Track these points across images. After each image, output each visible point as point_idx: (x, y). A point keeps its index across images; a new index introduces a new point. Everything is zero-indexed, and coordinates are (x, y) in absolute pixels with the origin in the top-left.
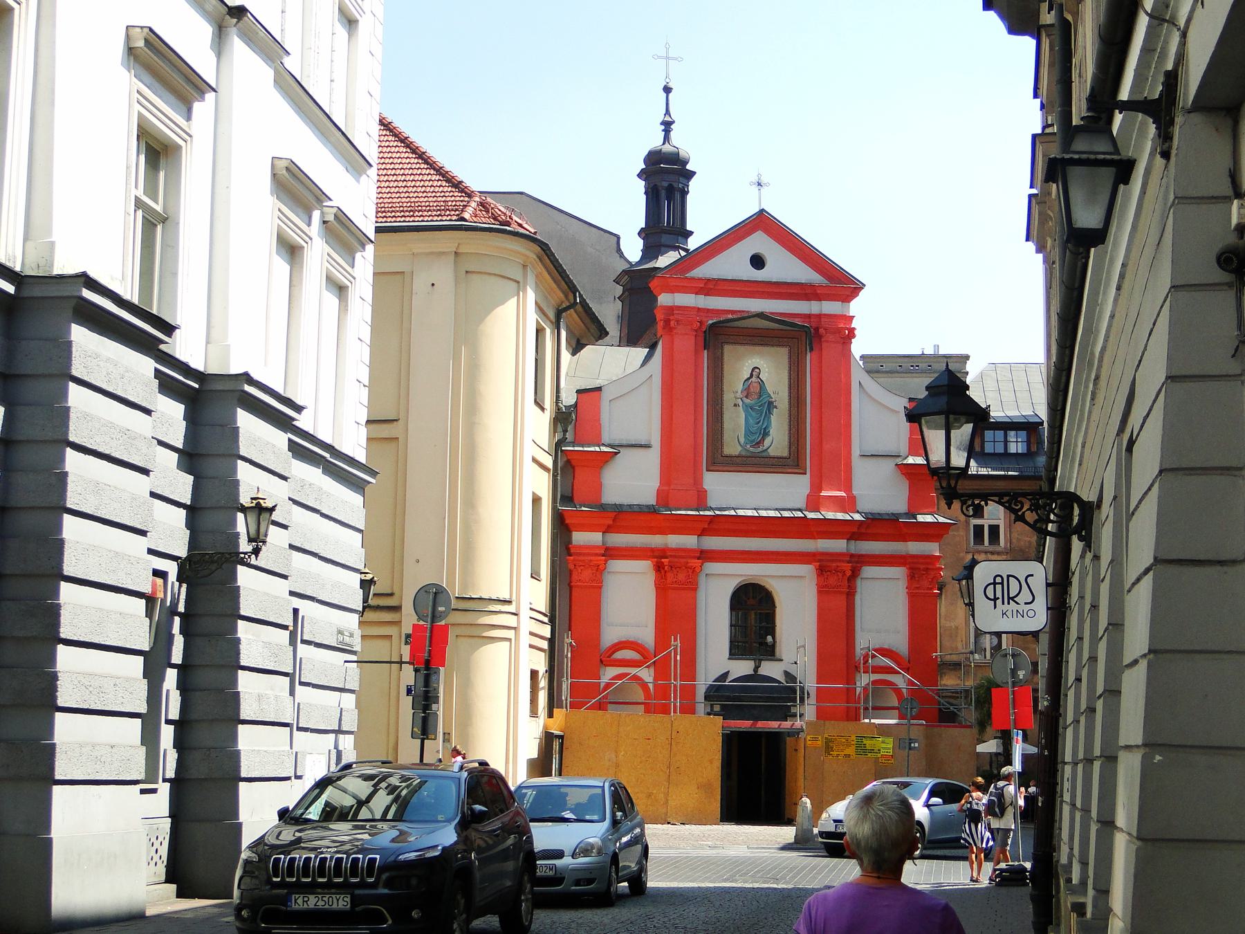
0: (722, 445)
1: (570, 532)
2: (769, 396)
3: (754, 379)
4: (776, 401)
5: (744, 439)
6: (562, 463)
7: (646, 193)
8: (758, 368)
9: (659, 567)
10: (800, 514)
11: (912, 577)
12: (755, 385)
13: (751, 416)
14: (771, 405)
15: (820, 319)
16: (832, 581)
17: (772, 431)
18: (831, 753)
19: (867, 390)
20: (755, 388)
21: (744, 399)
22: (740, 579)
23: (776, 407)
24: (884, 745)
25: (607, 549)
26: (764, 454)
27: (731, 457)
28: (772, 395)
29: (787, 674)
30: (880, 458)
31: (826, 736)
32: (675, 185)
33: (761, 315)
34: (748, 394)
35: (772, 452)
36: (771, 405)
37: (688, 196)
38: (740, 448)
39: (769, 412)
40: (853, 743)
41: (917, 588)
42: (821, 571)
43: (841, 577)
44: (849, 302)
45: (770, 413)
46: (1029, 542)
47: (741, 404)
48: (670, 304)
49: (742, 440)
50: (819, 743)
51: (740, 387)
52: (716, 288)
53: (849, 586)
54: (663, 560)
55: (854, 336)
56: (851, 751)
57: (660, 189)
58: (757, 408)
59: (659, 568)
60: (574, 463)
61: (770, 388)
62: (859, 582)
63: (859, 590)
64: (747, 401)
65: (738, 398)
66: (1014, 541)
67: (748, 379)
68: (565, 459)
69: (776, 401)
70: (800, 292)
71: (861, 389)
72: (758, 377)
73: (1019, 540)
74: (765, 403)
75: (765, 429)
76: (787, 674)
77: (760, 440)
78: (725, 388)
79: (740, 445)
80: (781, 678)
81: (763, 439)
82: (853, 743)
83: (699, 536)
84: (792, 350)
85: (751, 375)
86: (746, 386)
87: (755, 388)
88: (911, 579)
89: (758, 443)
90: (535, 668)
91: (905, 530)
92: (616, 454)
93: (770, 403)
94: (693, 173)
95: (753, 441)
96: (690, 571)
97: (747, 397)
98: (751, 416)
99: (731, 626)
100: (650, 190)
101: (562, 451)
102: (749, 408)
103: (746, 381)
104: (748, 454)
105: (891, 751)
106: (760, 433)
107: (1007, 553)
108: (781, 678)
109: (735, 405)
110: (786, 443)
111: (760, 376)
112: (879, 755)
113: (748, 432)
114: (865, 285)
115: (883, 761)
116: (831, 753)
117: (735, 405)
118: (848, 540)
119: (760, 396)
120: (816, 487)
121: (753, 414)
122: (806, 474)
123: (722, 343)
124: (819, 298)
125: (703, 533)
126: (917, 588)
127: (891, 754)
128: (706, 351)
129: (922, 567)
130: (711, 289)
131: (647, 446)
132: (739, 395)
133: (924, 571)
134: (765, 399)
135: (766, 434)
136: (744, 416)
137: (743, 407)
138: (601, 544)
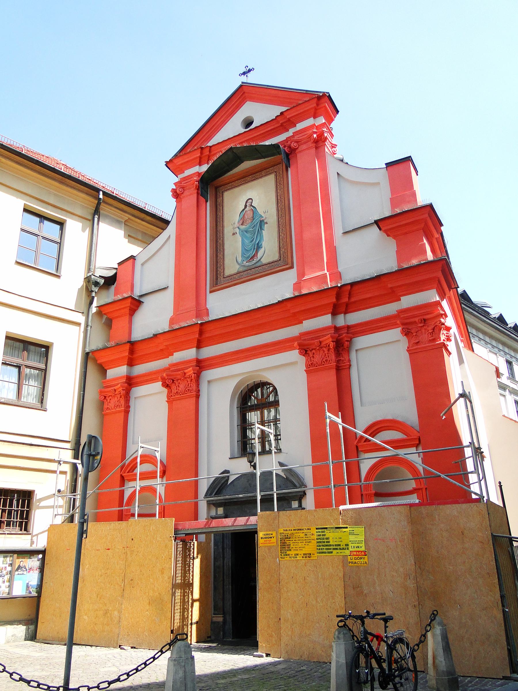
0: (224, 269)
2: (261, 217)
3: (248, 208)
5: (241, 258)
8: (252, 199)
13: (246, 237)
14: (262, 223)
16: (318, 358)
17: (264, 244)
18: (288, 552)
19: (346, 177)
20: (249, 214)
23: (267, 223)
24: (352, 538)
26: (259, 264)
28: (263, 215)
31: (281, 531)
34: (243, 222)
35: (264, 261)
36: (262, 223)
38: (238, 267)
39: (261, 228)
40: (312, 537)
42: (305, 351)
43: (326, 352)
47: (237, 230)
49: (240, 259)
50: (274, 540)
56: (311, 548)
58: (251, 229)
61: (260, 211)
63: (354, 363)
65: (236, 228)
67: (244, 210)
72: (251, 205)
74: (258, 222)
75: (258, 244)
77: (255, 254)
79: (239, 264)
81: (257, 252)
82: (312, 537)
89: (252, 258)
95: (249, 256)
97: (242, 224)
98: (246, 237)
102: (244, 233)
104: (245, 269)
105: (363, 544)
106: (254, 248)
109: (234, 234)
110: (276, 249)
111: (252, 205)
112: (347, 552)
113: (245, 251)
115: (354, 561)
116: (288, 552)
117: (234, 234)
119: (253, 219)
120: (301, 274)
121: (248, 235)
127: (363, 549)
132: (236, 225)
133: (421, 323)
134: (257, 220)
135: (258, 247)
137: (239, 233)
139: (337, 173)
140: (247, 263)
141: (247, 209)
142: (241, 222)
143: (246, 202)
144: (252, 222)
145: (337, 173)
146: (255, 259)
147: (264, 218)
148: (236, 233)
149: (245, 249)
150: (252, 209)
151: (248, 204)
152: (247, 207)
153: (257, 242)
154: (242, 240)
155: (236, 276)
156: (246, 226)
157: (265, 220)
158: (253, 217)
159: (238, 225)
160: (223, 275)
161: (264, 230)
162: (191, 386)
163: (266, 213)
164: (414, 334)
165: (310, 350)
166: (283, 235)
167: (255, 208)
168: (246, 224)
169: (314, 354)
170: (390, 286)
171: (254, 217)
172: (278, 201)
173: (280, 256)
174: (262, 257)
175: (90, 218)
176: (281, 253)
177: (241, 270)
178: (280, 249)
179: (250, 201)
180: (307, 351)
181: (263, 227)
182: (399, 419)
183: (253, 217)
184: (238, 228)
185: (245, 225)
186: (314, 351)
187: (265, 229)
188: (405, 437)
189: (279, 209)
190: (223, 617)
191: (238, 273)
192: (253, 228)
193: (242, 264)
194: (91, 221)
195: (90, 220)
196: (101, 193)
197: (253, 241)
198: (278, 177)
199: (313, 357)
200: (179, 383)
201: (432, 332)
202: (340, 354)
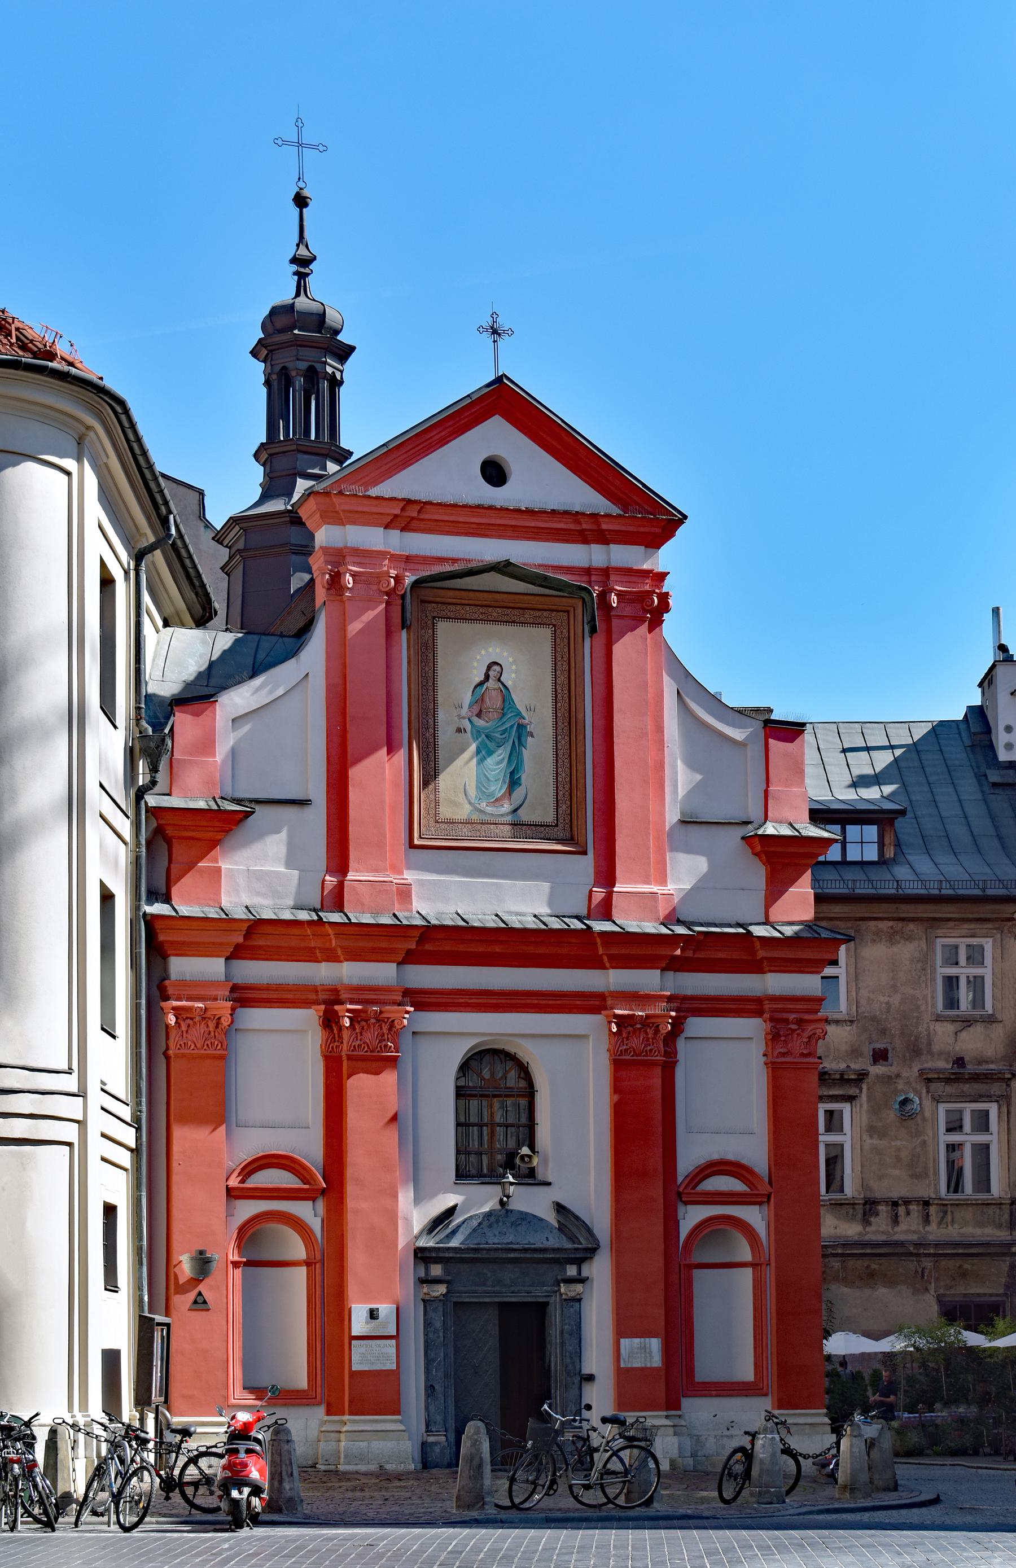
1: (165, 957)
3: (491, 684)
6: (149, 833)
7: (268, 383)
8: (501, 666)
9: (329, 1020)
10: (577, 925)
11: (774, 1037)
12: (494, 693)
15: (608, 577)
20: (493, 701)
21: (475, 719)
23: (532, 736)
25: (235, 988)
27: (451, 822)
28: (524, 713)
29: (560, 1208)
30: (714, 828)
32: (318, 366)
33: (504, 568)
34: (481, 711)
37: (342, 389)
38: (468, 808)
41: (783, 1054)
44: (658, 547)
46: (887, 1003)
47: (468, 727)
48: (340, 544)
49: (472, 793)
51: (467, 698)
52: (422, 516)
53: (665, 1051)
54: (336, 1007)
55: (667, 609)
57: (293, 373)
58: (498, 735)
59: (329, 1021)
60: (170, 832)
62: (681, 1044)
63: (680, 1056)
64: (480, 723)
65: (464, 718)
66: (863, 1002)
68: (154, 824)
70: (572, 526)
72: (499, 680)
73: (870, 1000)
74: (512, 727)
76: (560, 1208)
78: (441, 698)
79: (470, 803)
83: (399, 964)
84: (558, 631)
85: (487, 677)
86: (477, 696)
87: (493, 701)
88: (773, 1039)
90: (112, 1201)
91: (761, 954)
92: (248, 815)
93: (521, 727)
94: (352, 349)
95: (492, 795)
96: (385, 1028)
97: (479, 715)
99: (458, 1124)
100: (274, 377)
101: (148, 809)
103: (475, 687)
107: (852, 1022)
108: (551, 1217)
109: (459, 730)
111: (502, 679)
114: (685, 517)
117: (459, 730)
118: (663, 970)
119: (504, 714)
122: (585, 853)
123: (434, 618)
124: (603, 538)
125: (410, 958)
126: (783, 1054)
128: (404, 633)
129: (792, 1017)
130: (413, 519)
131: (303, 803)
138: (223, 979)
142: (476, 710)
143: (489, 668)
144: (501, 718)
146: (505, 805)
147: (527, 722)
149: (485, 775)
150: (501, 691)
151: (491, 673)
155: (465, 830)
156: (487, 722)
158: (503, 710)
159: (469, 713)
160: (436, 816)
162: (388, 1039)
163: (532, 712)
164: (783, 1038)
166: (564, 775)
167: (508, 689)
169: (629, 1033)
171: (505, 710)
172: (556, 697)
173: (557, 817)
174: (521, 806)
176: (560, 812)
177: (475, 817)
178: (557, 803)
179: (497, 668)
181: (523, 739)
182: (744, 1162)
183: (503, 710)
184: (469, 720)
185: (484, 720)
187: (528, 746)
188: (748, 1190)
189: (559, 715)
190: (445, 1435)
191: (467, 822)
193: (478, 806)
198: (558, 640)
200: (363, 1027)
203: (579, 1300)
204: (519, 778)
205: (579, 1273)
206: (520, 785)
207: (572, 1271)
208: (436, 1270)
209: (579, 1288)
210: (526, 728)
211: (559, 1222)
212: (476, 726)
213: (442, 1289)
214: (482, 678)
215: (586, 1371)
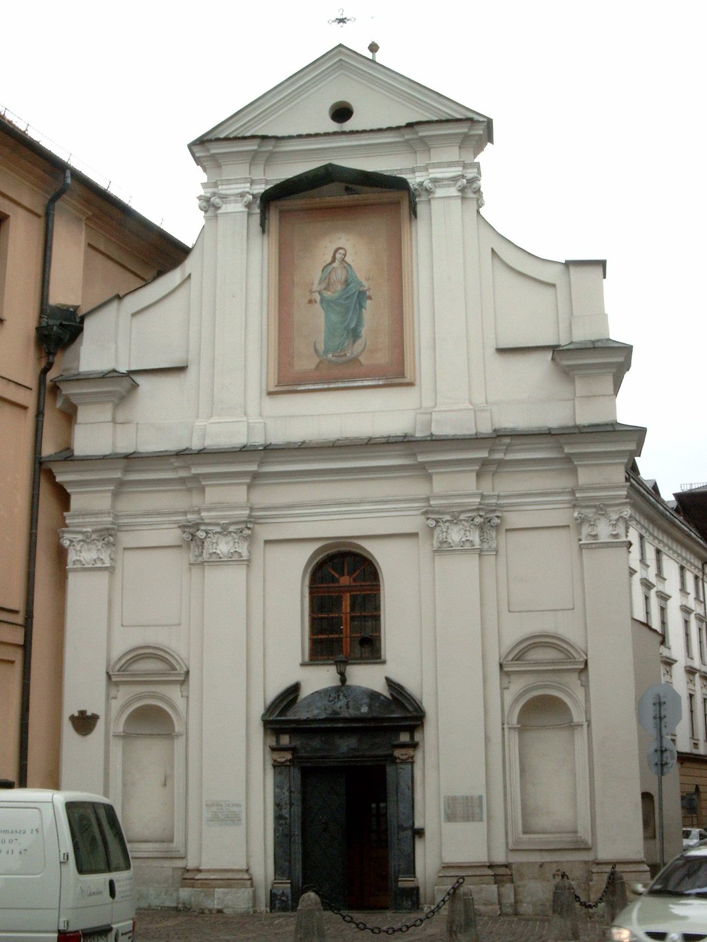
4: (369, 289)
8: (346, 251)
14: (362, 296)
17: (364, 331)
20: (339, 275)
21: (324, 292)
22: (318, 545)
23: (370, 298)
28: (365, 283)
29: (390, 683)
34: (329, 285)
45: (361, 307)
49: (321, 347)
51: (317, 275)
58: (342, 302)
69: (369, 289)
71: (496, 261)
74: (356, 292)
80: (380, 687)
85: (334, 259)
103: (325, 267)
109: (310, 302)
117: (310, 302)
132: (316, 287)
136: (323, 314)
139: (492, 249)
140: (333, 358)
141: (334, 265)
142: (324, 285)
145: (492, 249)
147: (366, 288)
148: (316, 302)
151: (338, 256)
152: (336, 261)
153: (353, 325)
154: (327, 318)
156: (334, 293)
157: (368, 292)
161: (365, 309)
165: (442, 521)
168: (333, 290)
170: (567, 450)
175: (40, 211)
179: (341, 251)
180: (439, 522)
184: (320, 293)
186: (447, 524)
190: (290, 883)
192: (345, 301)
194: (43, 219)
195: (39, 216)
196: (68, 173)
197: (345, 321)
199: (447, 532)
201: (615, 524)
202: (483, 532)
203: (412, 763)
204: (361, 331)
205: (412, 737)
206: (361, 337)
207: (404, 738)
208: (285, 740)
209: (410, 752)
210: (366, 294)
211: (391, 695)
212: (324, 297)
213: (288, 756)
214: (329, 260)
215: (418, 825)
